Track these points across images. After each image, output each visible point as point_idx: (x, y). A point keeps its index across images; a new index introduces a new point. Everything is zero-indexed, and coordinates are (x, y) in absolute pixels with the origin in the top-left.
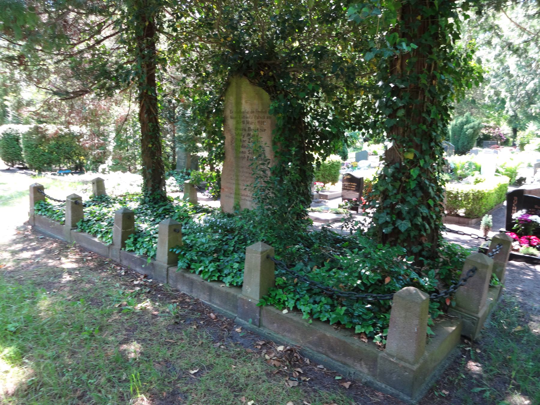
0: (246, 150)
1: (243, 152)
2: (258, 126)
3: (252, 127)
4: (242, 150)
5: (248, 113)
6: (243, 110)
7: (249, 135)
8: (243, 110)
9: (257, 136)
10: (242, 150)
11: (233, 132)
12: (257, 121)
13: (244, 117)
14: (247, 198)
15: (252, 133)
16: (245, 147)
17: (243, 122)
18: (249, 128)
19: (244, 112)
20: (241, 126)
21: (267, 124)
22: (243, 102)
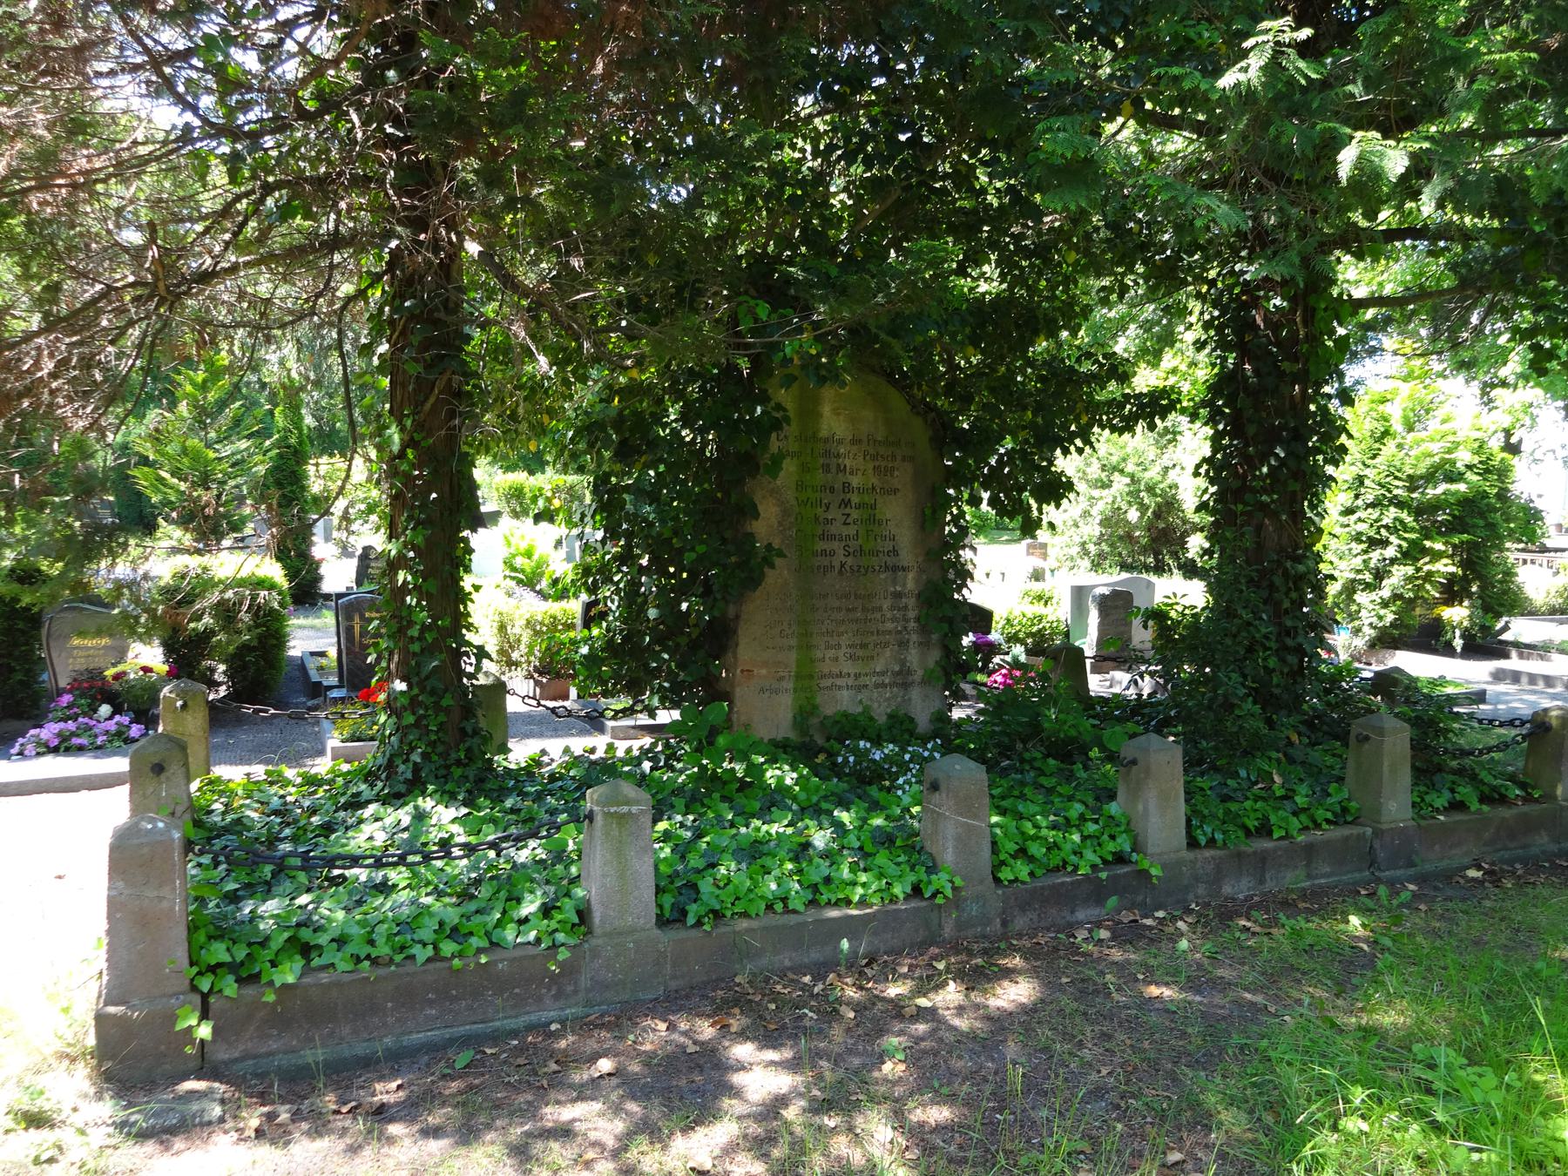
0: (835, 545)
1: (824, 553)
2: (875, 481)
3: (855, 481)
4: (820, 546)
5: (840, 442)
6: (824, 433)
7: (846, 503)
8: (824, 433)
9: (874, 507)
10: (820, 546)
11: (790, 495)
12: (871, 466)
13: (827, 454)
14: (839, 682)
15: (855, 499)
16: (833, 537)
17: (826, 468)
18: (847, 487)
19: (826, 440)
20: (819, 478)
21: (902, 476)
22: (826, 410)
